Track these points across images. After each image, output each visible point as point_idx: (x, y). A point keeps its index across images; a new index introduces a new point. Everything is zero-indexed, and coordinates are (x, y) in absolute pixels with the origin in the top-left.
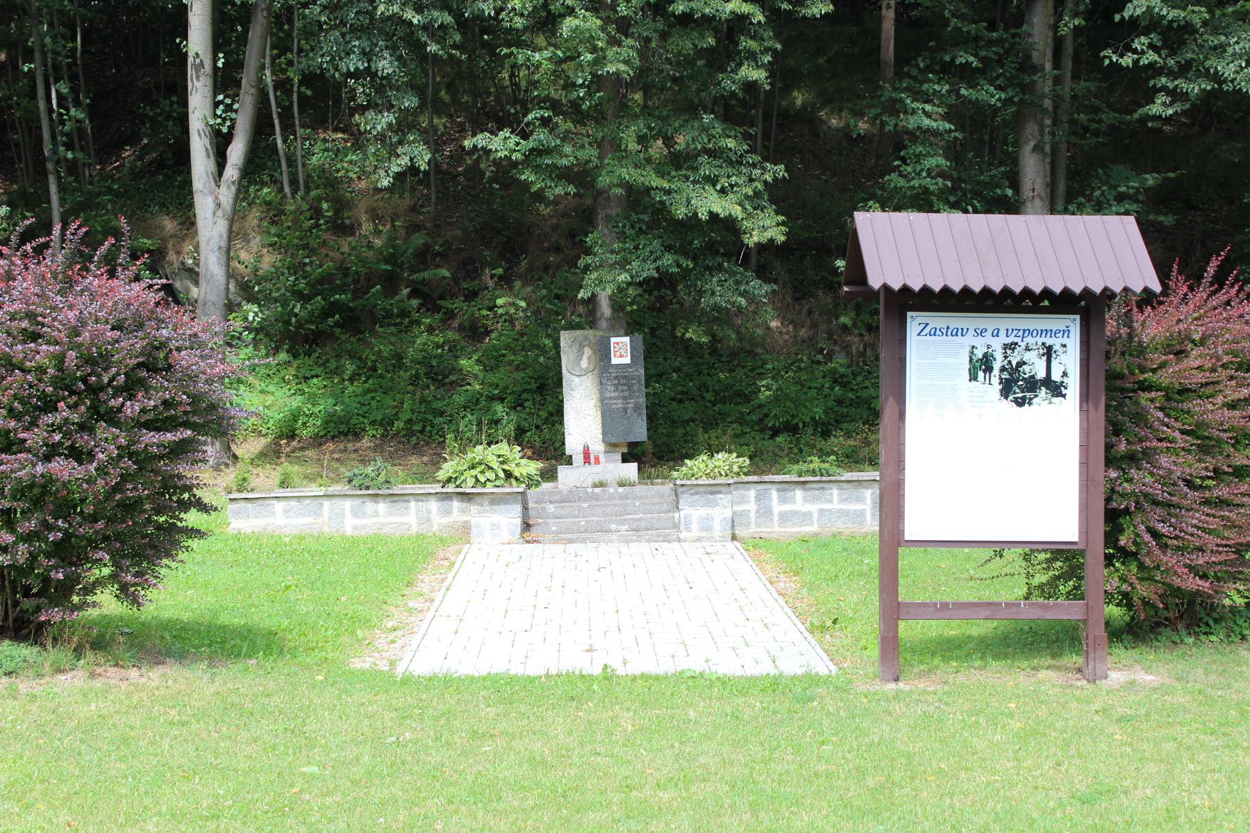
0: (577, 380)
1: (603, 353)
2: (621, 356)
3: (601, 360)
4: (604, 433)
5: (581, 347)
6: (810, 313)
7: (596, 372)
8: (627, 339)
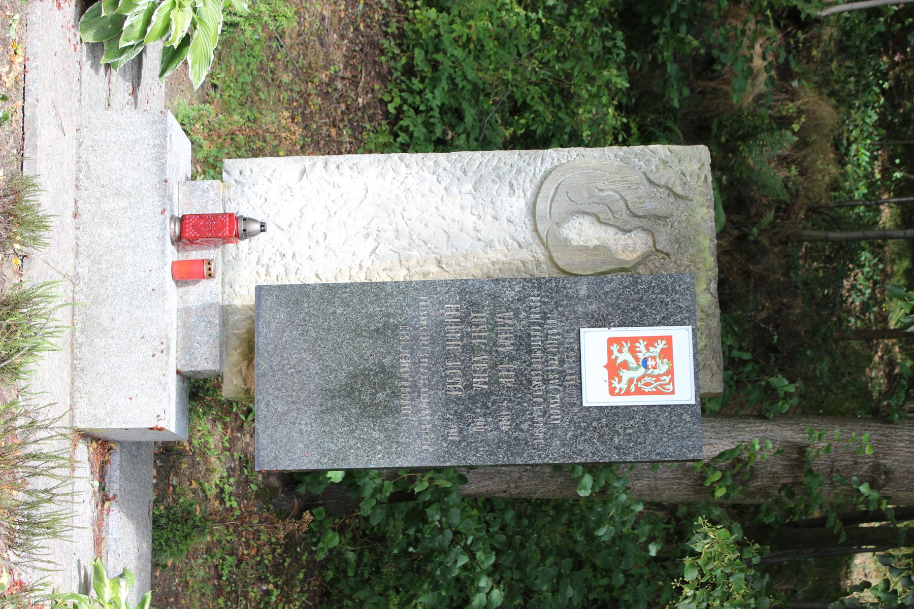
0: (517, 205)
2: (613, 368)
5: (652, 221)
7: (546, 272)
8: (684, 392)
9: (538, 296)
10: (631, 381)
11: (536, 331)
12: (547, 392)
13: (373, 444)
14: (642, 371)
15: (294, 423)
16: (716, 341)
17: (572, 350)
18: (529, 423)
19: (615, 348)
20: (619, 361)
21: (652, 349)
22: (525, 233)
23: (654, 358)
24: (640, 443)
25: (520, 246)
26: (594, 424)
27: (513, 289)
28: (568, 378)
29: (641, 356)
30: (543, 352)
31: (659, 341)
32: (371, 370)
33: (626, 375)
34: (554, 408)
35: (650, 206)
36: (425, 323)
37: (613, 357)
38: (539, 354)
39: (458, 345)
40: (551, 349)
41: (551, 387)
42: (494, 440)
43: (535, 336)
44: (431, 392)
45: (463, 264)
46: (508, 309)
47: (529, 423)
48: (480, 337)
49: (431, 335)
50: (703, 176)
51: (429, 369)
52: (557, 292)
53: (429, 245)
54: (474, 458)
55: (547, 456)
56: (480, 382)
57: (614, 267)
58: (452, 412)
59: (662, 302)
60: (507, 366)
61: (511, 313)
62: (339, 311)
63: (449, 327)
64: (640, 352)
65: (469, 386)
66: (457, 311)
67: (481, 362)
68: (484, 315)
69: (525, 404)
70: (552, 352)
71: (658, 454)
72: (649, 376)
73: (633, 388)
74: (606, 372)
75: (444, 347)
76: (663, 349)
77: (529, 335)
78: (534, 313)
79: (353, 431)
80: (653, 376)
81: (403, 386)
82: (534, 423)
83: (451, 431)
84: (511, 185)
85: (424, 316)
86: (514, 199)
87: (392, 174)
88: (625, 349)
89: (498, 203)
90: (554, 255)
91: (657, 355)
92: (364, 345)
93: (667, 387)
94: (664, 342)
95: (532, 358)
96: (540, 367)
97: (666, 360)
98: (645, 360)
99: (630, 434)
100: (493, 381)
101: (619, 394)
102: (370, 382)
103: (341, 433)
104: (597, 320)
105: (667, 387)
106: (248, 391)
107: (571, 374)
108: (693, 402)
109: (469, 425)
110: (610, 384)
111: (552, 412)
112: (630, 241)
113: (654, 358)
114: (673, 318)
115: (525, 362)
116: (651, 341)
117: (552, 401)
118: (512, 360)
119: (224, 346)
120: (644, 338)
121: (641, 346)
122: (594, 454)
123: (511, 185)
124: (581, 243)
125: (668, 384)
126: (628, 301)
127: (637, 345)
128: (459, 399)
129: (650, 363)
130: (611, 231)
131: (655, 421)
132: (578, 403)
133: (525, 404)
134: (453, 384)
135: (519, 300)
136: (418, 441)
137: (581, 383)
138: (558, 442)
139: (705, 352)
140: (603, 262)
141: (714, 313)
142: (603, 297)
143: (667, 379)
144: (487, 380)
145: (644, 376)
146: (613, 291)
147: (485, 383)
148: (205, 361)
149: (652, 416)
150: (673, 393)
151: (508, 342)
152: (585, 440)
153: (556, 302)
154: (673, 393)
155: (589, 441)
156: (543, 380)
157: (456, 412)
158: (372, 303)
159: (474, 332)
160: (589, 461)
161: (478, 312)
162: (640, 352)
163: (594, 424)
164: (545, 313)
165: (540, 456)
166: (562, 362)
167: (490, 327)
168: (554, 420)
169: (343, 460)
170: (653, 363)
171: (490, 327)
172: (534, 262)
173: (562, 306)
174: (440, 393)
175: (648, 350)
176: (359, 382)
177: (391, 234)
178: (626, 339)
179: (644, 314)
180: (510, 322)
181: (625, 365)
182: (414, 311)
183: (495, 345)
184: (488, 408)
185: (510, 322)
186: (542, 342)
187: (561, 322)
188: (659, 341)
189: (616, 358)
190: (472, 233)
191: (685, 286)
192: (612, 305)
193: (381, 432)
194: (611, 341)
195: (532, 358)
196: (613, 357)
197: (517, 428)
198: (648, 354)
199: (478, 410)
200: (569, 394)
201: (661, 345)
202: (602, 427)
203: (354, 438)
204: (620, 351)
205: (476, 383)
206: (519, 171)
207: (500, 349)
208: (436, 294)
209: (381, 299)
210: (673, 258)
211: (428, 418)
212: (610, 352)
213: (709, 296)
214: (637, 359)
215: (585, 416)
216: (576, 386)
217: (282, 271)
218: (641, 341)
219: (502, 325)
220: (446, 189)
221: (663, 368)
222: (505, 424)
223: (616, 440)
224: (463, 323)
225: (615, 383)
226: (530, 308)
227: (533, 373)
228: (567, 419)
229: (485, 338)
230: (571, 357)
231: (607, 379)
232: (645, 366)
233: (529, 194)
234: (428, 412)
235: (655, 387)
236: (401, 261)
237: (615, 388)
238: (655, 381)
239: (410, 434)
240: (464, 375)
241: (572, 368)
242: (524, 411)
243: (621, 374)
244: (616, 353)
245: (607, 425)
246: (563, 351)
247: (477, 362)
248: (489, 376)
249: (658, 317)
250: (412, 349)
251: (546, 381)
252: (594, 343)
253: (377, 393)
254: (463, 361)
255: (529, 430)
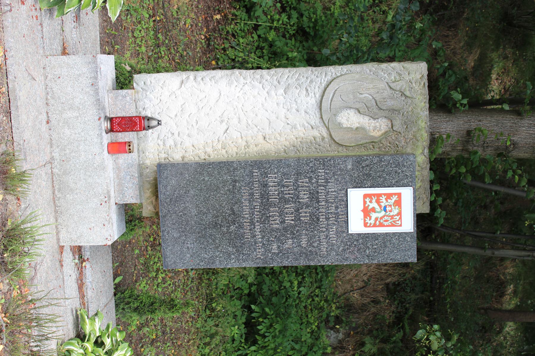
0: (312, 101)
1: (374, 167)
2: (367, 212)
3: (359, 161)
4: (182, 167)
5: (391, 113)
6: (375, 302)
8: (408, 225)
9: (323, 169)
10: (376, 219)
11: (321, 190)
12: (328, 225)
13: (229, 255)
14: (383, 213)
15: (184, 243)
16: (426, 183)
17: (343, 201)
18: (318, 242)
19: (368, 200)
20: (370, 208)
21: (389, 201)
22: (315, 120)
23: (390, 206)
24: (381, 253)
25: (312, 128)
26: (355, 243)
27: (308, 165)
28: (340, 217)
29: (383, 205)
30: (326, 202)
31: (394, 196)
32: (227, 213)
33: (374, 215)
34: (332, 234)
35: (390, 103)
36: (257, 185)
37: (367, 205)
38: (323, 203)
39: (276, 198)
40: (330, 200)
41: (330, 222)
42: (298, 252)
43: (321, 193)
44: (261, 225)
45: (279, 139)
46: (306, 177)
47: (318, 242)
48: (289, 194)
49: (261, 193)
50: (423, 83)
51: (260, 212)
52: (334, 167)
53: (258, 127)
54: (286, 262)
55: (328, 261)
56: (289, 220)
57: (368, 141)
58: (274, 237)
59: (396, 172)
60: (305, 210)
61: (307, 180)
62: (206, 179)
63: (271, 188)
64: (382, 202)
65: (283, 222)
66: (275, 178)
67: (290, 207)
68: (291, 181)
69: (316, 232)
70: (331, 202)
71: (391, 259)
72: (387, 216)
73: (378, 223)
74: (362, 214)
75: (268, 200)
76: (396, 200)
77: (318, 192)
78: (321, 179)
79: (217, 247)
80: (389, 216)
81: (245, 222)
82: (321, 242)
83: (273, 247)
84: (307, 90)
85: (256, 181)
86: (309, 98)
87: (236, 83)
88: (374, 201)
89: (299, 101)
90: (333, 134)
91: (392, 204)
92: (222, 199)
93: (397, 222)
94: (396, 197)
95: (320, 206)
96: (324, 210)
97: (397, 207)
98: (385, 207)
99: (375, 248)
100: (297, 218)
101: (369, 227)
102: (226, 219)
103: (211, 249)
104: (357, 183)
105: (397, 222)
106: (157, 214)
107: (342, 215)
108: (412, 231)
109: (283, 244)
110: (365, 220)
111: (331, 236)
112: (378, 124)
113: (390, 206)
114: (402, 182)
115: (315, 208)
116: (389, 196)
117: (331, 230)
118: (307, 207)
119: (141, 188)
120: (385, 194)
121: (383, 199)
122: (354, 259)
123: (307, 90)
124: (349, 126)
125: (398, 220)
126: (376, 172)
127: (381, 198)
128: (278, 229)
129: (388, 209)
130: (367, 118)
131: (390, 241)
132: (346, 231)
133: (316, 232)
134: (274, 221)
135: (312, 172)
136: (255, 253)
137: (348, 220)
138: (334, 253)
139: (419, 190)
140: (361, 138)
141: (426, 167)
142: (361, 169)
143: (398, 218)
144: (293, 218)
145: (384, 217)
146: (367, 166)
147: (292, 220)
148: (131, 197)
149: (388, 238)
150: (401, 226)
151: (306, 197)
152: (350, 252)
153: (334, 173)
154: (401, 226)
155: (352, 253)
156: (326, 218)
157: (276, 236)
158: (225, 174)
159: (286, 191)
160: (352, 263)
161: (288, 179)
162: (382, 202)
163: (355, 243)
164: (327, 179)
165: (324, 261)
166: (337, 208)
167: (295, 188)
168: (332, 241)
169: (212, 263)
170: (390, 209)
171: (295, 188)
172: (321, 137)
173: (337, 175)
174: (266, 226)
175: (387, 201)
176: (220, 220)
177: (235, 121)
178: (374, 195)
179: (385, 179)
180: (307, 185)
181: (373, 210)
182: (250, 179)
183: (298, 198)
184: (294, 234)
185: (307, 185)
186: (325, 196)
187: (336, 184)
188: (394, 196)
189: (369, 205)
190: (284, 119)
191: (410, 163)
192: (366, 174)
193: (233, 247)
194: (365, 196)
195: (320, 206)
196: (367, 205)
197: (311, 245)
198: (387, 204)
199: (288, 236)
200: (341, 226)
201: (395, 198)
202: (359, 244)
203: (218, 251)
204: (371, 202)
205: (287, 220)
206: (311, 81)
207: (301, 200)
208: (263, 168)
209: (231, 171)
210: (403, 134)
211: (260, 240)
212: (365, 203)
213: (424, 157)
214: (380, 206)
215: (350, 238)
216: (344, 221)
217: (173, 144)
218: (383, 196)
219: (302, 187)
220: (268, 93)
221: (395, 211)
222: (304, 243)
223: (367, 252)
224: (279, 185)
225: (368, 220)
226: (318, 177)
227: (320, 214)
228: (339, 240)
229: (292, 194)
230: (342, 205)
231: (363, 218)
232: (385, 211)
233: (317, 96)
234: (260, 237)
235: (391, 223)
236: (242, 137)
237: (367, 223)
238: (391, 219)
239: (250, 249)
240: (280, 215)
241: (342, 211)
242: (315, 236)
243: (371, 215)
244: (368, 203)
245: (362, 243)
246: (338, 202)
247: (288, 208)
248: (295, 216)
249: (393, 181)
250: (250, 201)
251: (327, 219)
252: (356, 197)
253: (230, 226)
254: (279, 208)
255: (317, 246)
